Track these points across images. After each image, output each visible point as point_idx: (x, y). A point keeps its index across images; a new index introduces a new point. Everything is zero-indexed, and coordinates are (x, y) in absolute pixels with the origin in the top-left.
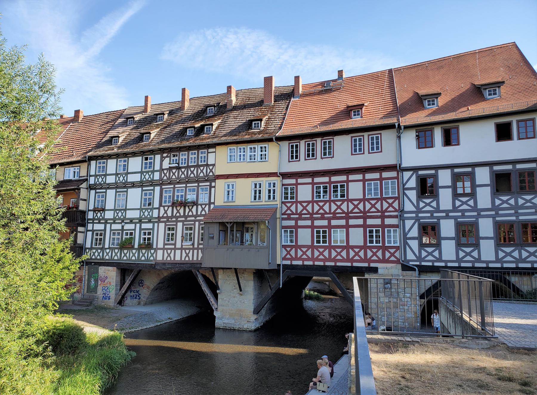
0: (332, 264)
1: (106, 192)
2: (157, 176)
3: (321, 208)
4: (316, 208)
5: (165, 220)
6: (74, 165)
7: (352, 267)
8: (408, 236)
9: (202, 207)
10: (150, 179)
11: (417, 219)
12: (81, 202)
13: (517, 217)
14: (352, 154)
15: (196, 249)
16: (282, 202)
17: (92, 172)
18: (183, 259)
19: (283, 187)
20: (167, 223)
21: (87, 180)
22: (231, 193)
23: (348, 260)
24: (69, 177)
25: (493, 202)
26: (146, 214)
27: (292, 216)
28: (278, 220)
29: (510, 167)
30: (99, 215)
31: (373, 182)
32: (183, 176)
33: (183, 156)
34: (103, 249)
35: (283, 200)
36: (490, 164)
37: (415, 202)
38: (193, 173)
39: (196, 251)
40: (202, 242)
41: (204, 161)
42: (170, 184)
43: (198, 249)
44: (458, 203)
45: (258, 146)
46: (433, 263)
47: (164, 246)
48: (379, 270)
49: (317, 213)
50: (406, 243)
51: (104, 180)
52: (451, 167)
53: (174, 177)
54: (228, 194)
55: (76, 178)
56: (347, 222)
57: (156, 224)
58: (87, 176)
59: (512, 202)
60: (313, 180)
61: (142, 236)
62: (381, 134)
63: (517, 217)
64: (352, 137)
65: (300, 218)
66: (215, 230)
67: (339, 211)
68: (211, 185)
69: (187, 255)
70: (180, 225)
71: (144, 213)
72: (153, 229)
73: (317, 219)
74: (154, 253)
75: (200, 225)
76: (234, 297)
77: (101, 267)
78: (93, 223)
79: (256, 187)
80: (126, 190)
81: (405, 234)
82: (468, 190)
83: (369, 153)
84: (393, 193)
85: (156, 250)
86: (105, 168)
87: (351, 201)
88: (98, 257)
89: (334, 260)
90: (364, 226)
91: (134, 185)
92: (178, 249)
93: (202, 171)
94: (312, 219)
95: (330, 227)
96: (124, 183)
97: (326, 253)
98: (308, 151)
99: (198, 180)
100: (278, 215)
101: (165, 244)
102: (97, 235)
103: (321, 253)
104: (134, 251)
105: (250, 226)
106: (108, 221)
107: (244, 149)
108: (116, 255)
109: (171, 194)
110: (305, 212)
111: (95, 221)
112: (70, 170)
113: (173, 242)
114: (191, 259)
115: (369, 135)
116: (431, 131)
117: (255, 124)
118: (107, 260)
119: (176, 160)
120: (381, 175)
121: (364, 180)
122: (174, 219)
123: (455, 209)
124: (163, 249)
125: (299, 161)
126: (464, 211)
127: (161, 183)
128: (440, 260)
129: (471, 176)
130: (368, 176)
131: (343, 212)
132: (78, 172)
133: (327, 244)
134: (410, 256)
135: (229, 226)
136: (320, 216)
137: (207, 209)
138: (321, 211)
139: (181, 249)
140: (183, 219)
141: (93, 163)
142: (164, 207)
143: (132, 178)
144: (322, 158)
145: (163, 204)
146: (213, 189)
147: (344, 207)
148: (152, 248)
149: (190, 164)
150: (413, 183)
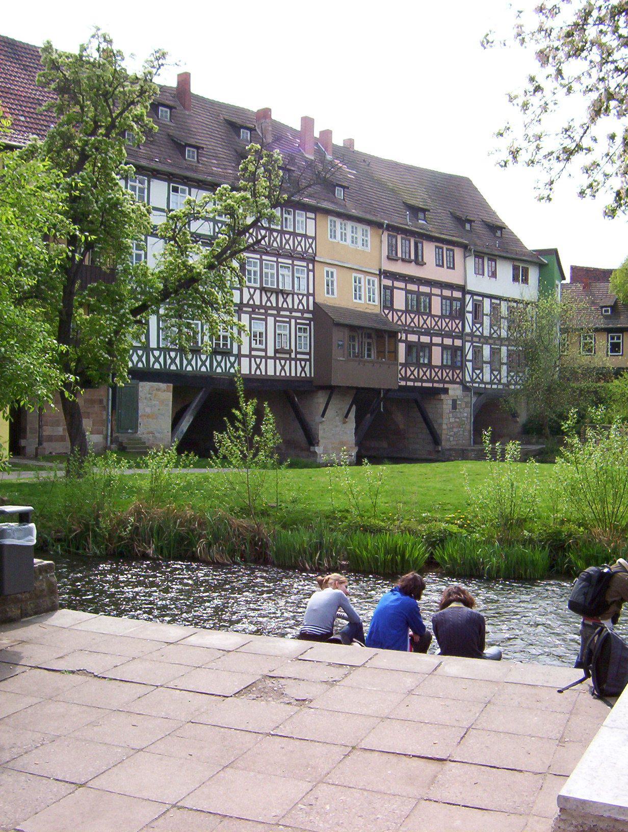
5: (251, 310)
7: (433, 388)
9: (299, 298)
11: (472, 342)
15: (293, 359)
20: (253, 316)
34: (146, 348)
37: (471, 326)
39: (293, 363)
43: (296, 359)
47: (250, 352)
48: (450, 391)
52: (491, 297)
69: (283, 368)
70: (271, 320)
75: (296, 324)
76: (336, 426)
77: (144, 383)
81: (466, 356)
85: (239, 356)
88: (140, 365)
92: (271, 358)
93: (299, 243)
99: (291, 255)
101: (251, 349)
109: (258, 269)
113: (264, 347)
114: (288, 374)
124: (250, 356)
134: (468, 379)
137: (304, 301)
140: (275, 312)
142: (249, 288)
146: (311, 274)
148: (234, 355)
149: (284, 229)
150: (469, 308)
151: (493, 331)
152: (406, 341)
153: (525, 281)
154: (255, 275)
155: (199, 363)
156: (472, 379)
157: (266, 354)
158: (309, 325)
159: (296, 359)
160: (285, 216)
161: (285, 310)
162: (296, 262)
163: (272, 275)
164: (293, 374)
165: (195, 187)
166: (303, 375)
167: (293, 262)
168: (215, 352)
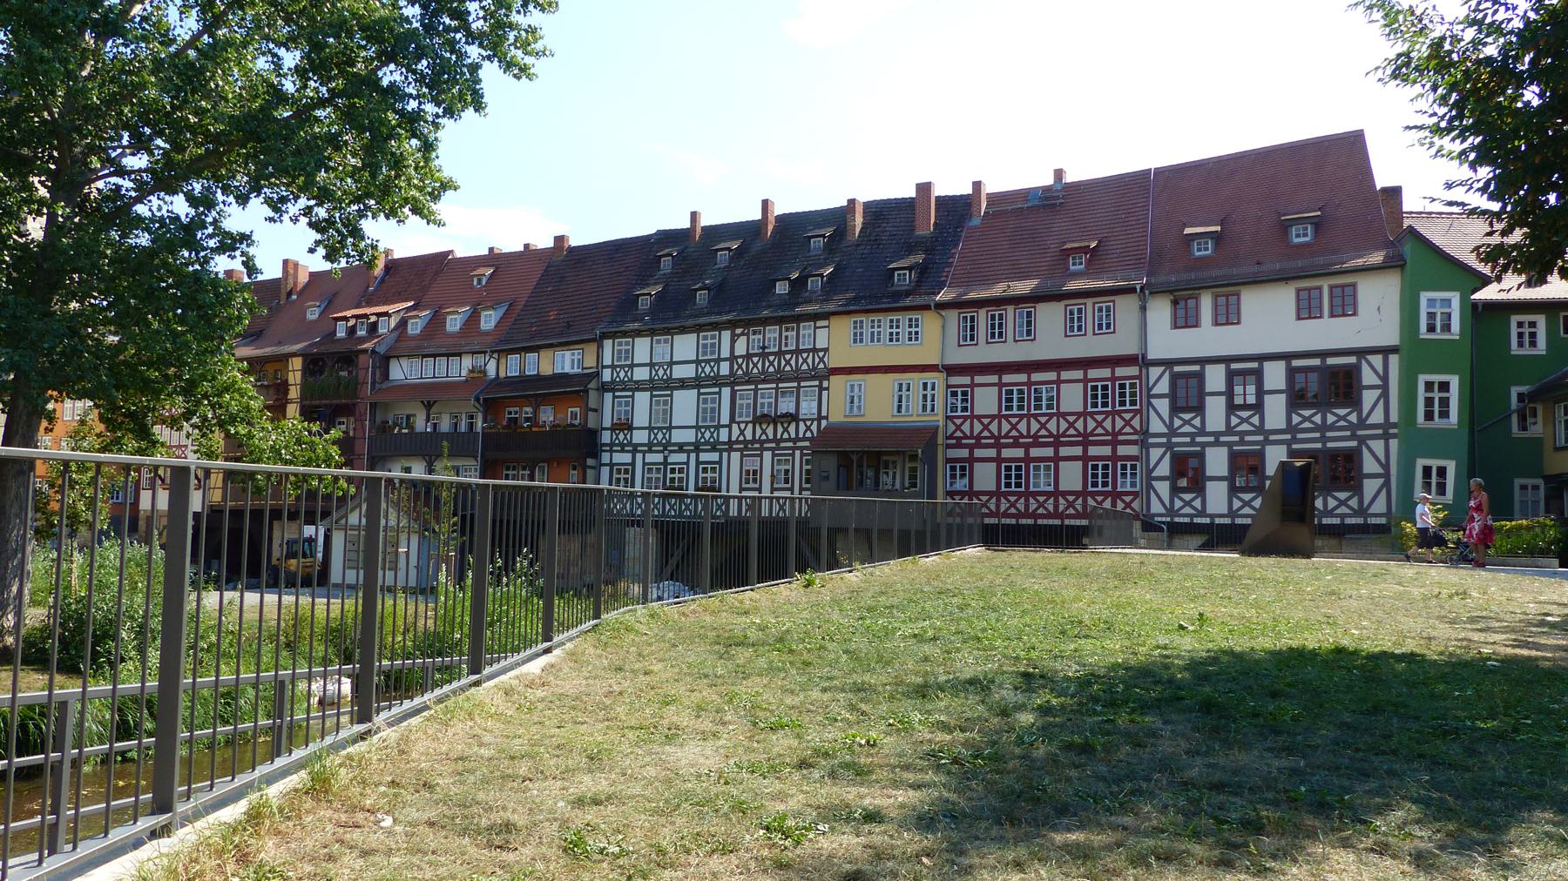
0: (1030, 521)
1: (633, 397)
2: (725, 369)
3: (1014, 427)
4: (1006, 427)
5: (742, 446)
6: (571, 347)
8: (1154, 474)
10: (712, 374)
11: (1169, 446)
12: (590, 413)
13: (1324, 444)
14: (1066, 336)
16: (947, 417)
17: (607, 361)
19: (949, 390)
21: (597, 375)
22: (856, 400)
23: (1056, 514)
24: (563, 369)
25: (1289, 420)
26: (707, 435)
27: (964, 441)
28: (940, 450)
29: (1316, 362)
30: (621, 436)
31: (1100, 384)
32: (771, 369)
33: (772, 332)
35: (949, 414)
36: (1286, 357)
37: (1166, 418)
38: (790, 364)
40: (808, 486)
41: (809, 344)
42: (748, 382)
44: (1235, 421)
45: (905, 318)
46: (1192, 519)
49: (1006, 436)
50: (1150, 487)
51: (629, 374)
53: (755, 371)
54: (852, 402)
55: (576, 370)
56: (1057, 452)
57: (725, 455)
58: (597, 367)
59: (1318, 419)
60: (1000, 379)
61: (701, 475)
62: (1113, 301)
63: (1324, 444)
64: (1066, 306)
65: (979, 445)
66: (830, 464)
67: (1043, 432)
68: (821, 384)
70: (767, 455)
71: (703, 434)
72: (720, 462)
73: (1007, 446)
75: (802, 455)
78: (611, 451)
79: (900, 390)
81: (1150, 471)
82: (1251, 400)
83: (1094, 334)
84: (1133, 403)
86: (630, 353)
87: (1064, 415)
89: (1035, 516)
90: (1085, 458)
91: (683, 384)
93: (805, 361)
94: (999, 446)
95: (1028, 459)
96: (665, 381)
97: (1021, 505)
98: (993, 326)
99: (798, 376)
100: (940, 440)
102: (619, 471)
103: (1013, 505)
105: (891, 458)
106: (639, 448)
107: (879, 321)
109: (751, 401)
110: (986, 434)
111: (615, 448)
112: (563, 356)
113: (757, 486)
115: (1094, 304)
116: (1196, 298)
117: (899, 275)
119: (759, 340)
120: (1113, 372)
121: (1085, 381)
122: (757, 446)
123: (1230, 430)
125: (977, 344)
126: (1243, 434)
127: (732, 381)
128: (1202, 513)
129: (1258, 375)
130: (1093, 373)
131: (1051, 435)
132: (579, 360)
133: (1023, 489)
134: (1156, 507)
135: (855, 458)
136: (1011, 440)
137: (814, 428)
138: (1014, 433)
140: (773, 445)
141: (608, 344)
142: (739, 423)
143: (680, 372)
144: (1015, 341)
146: (825, 393)
147: (1052, 426)
149: (783, 349)
150: (1163, 387)
160: (784, 334)
165: (677, 334)
167: (799, 384)
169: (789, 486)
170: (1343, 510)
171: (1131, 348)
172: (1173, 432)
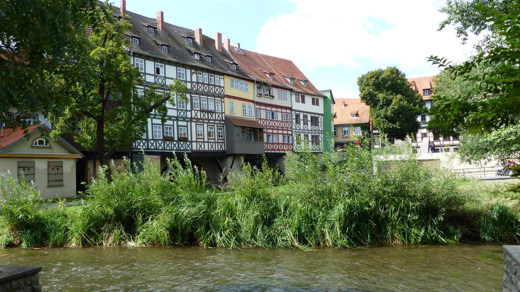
2: (189, 86)
4: (268, 123)
5: (196, 120)
15: (217, 142)
18: (210, 149)
23: (279, 150)
26: (182, 114)
33: (206, 75)
34: (147, 140)
39: (217, 144)
42: (197, 94)
43: (218, 142)
53: (194, 89)
57: (189, 123)
67: (275, 126)
68: (221, 100)
70: (205, 125)
71: (180, 113)
72: (187, 126)
74: (189, 144)
75: (217, 126)
80: (163, 91)
85: (191, 142)
90: (283, 134)
92: (206, 142)
93: (217, 90)
96: (162, 85)
99: (214, 95)
101: (197, 139)
104: (175, 143)
108: (160, 145)
109: (198, 102)
114: (214, 149)
118: (153, 149)
121: (282, 112)
122: (201, 121)
124: (196, 142)
126: (306, 130)
127: (191, 92)
133: (272, 142)
134: (295, 148)
137: (220, 116)
138: (269, 125)
139: (208, 142)
140: (207, 121)
142: (195, 110)
145: (194, 109)
146: (223, 103)
148: (189, 141)
150: (294, 117)
151: (304, 127)
152: (267, 133)
153: (318, 104)
154: (197, 104)
155: (173, 146)
156: (296, 148)
157: (204, 140)
158: (223, 127)
159: (218, 142)
160: (210, 77)
161: (212, 120)
162: (216, 99)
163: (205, 104)
164: (217, 149)
165: (167, 64)
166: (221, 149)
167: (214, 98)
168: (180, 139)
169: (214, 138)
170: (318, 149)
171: (290, 106)
172: (296, 129)
